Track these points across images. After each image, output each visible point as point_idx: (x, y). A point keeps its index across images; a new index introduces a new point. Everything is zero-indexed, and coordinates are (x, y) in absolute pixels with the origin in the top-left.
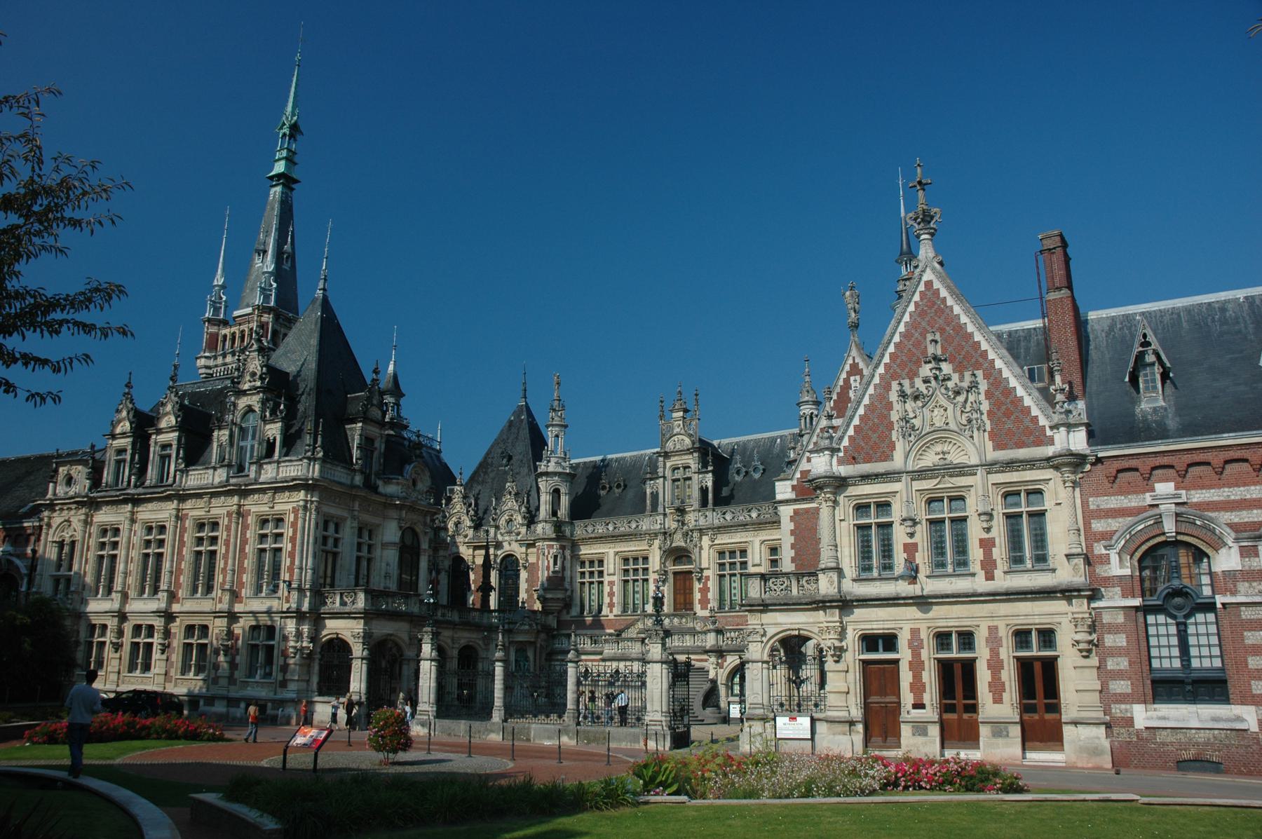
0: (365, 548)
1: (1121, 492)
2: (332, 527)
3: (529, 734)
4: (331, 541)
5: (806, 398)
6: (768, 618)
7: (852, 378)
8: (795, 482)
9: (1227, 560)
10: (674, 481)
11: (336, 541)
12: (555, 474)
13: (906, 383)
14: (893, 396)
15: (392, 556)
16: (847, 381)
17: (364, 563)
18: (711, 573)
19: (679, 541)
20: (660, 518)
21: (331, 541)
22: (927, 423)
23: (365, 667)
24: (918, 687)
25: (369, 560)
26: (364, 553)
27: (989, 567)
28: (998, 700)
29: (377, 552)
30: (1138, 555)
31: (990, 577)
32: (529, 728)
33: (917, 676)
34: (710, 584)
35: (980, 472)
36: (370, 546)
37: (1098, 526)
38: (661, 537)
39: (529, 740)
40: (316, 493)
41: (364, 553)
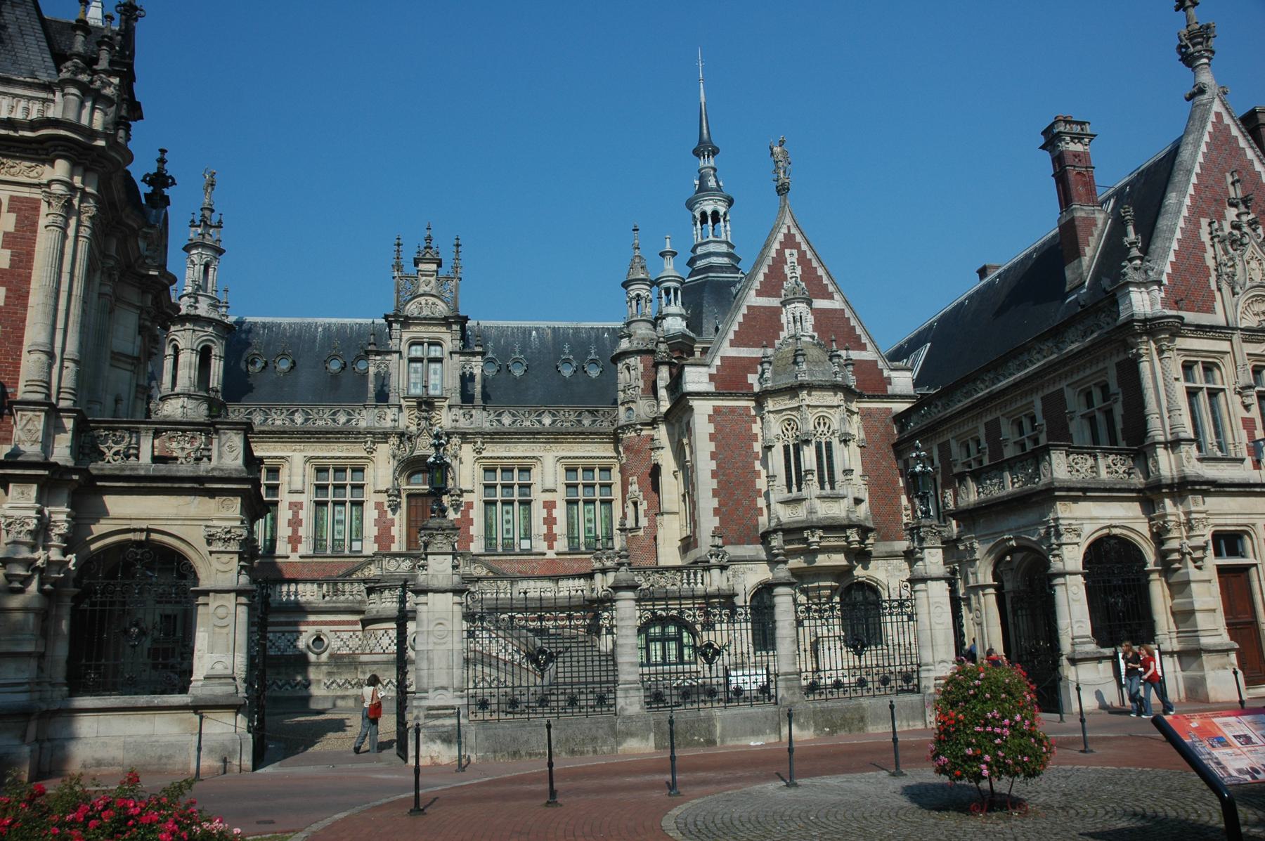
3: (710, 730)
5: (642, 276)
7: (787, 252)
8: (714, 371)
10: (412, 360)
12: (209, 321)
14: (1205, 237)
16: (780, 253)
18: (477, 499)
19: (424, 447)
20: (391, 413)
23: (243, 612)
32: (710, 719)
34: (472, 514)
38: (394, 440)
39: (711, 742)
40: (93, 177)
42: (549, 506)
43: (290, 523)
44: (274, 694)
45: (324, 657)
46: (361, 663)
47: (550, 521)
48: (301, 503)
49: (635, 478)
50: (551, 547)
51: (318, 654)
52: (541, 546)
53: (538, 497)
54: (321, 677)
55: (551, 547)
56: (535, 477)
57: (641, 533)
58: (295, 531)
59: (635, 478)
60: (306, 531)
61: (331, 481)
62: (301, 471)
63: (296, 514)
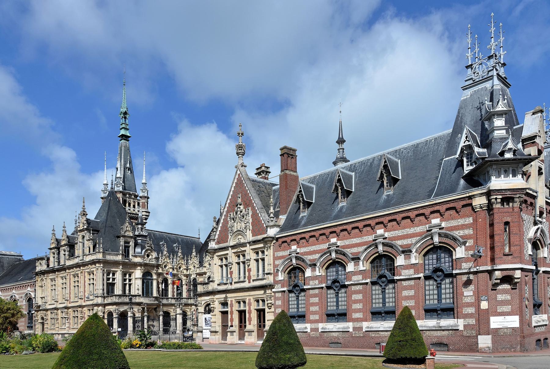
0: (128, 281)
1: (284, 250)
2: (111, 275)
4: (111, 280)
6: (203, 298)
9: (308, 273)
11: (114, 279)
13: (232, 214)
15: (139, 282)
17: (127, 286)
21: (111, 280)
22: (236, 228)
24: (232, 320)
25: (130, 285)
26: (127, 281)
27: (249, 277)
28: (250, 324)
29: (133, 282)
30: (287, 272)
31: (249, 282)
33: (232, 316)
35: (248, 245)
36: (130, 280)
37: (277, 262)
41: (127, 281)
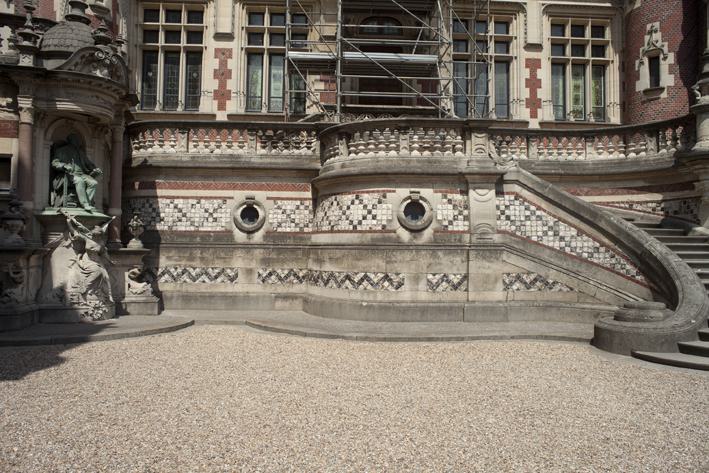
42: (533, 65)
43: (217, 74)
44: (184, 288)
45: (258, 237)
46: (316, 246)
47: (533, 83)
48: (230, 50)
49: (657, 25)
50: (534, 115)
51: (250, 232)
52: (521, 113)
53: (517, 50)
54: (253, 265)
55: (534, 115)
56: (516, 28)
57: (664, 95)
58: (223, 85)
59: (657, 25)
60: (236, 84)
61: (266, 45)
62: (230, 9)
63: (223, 64)
